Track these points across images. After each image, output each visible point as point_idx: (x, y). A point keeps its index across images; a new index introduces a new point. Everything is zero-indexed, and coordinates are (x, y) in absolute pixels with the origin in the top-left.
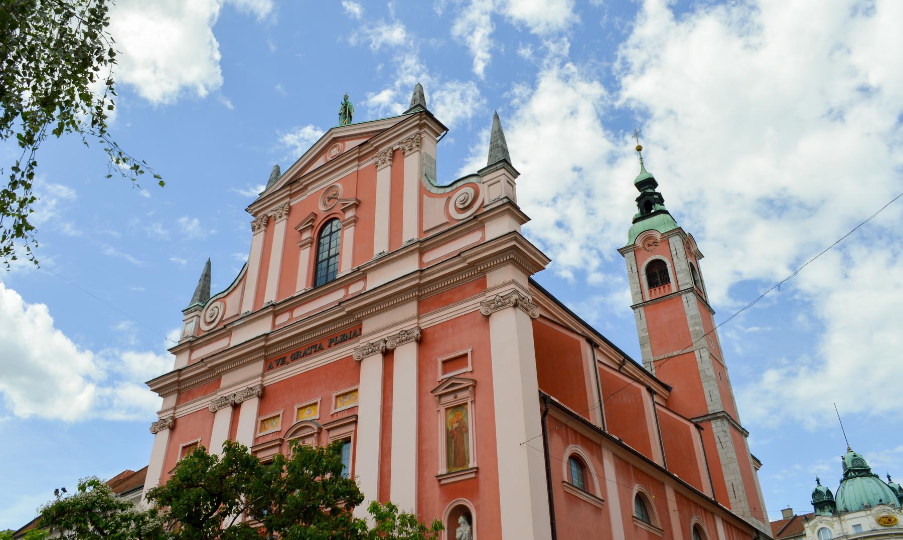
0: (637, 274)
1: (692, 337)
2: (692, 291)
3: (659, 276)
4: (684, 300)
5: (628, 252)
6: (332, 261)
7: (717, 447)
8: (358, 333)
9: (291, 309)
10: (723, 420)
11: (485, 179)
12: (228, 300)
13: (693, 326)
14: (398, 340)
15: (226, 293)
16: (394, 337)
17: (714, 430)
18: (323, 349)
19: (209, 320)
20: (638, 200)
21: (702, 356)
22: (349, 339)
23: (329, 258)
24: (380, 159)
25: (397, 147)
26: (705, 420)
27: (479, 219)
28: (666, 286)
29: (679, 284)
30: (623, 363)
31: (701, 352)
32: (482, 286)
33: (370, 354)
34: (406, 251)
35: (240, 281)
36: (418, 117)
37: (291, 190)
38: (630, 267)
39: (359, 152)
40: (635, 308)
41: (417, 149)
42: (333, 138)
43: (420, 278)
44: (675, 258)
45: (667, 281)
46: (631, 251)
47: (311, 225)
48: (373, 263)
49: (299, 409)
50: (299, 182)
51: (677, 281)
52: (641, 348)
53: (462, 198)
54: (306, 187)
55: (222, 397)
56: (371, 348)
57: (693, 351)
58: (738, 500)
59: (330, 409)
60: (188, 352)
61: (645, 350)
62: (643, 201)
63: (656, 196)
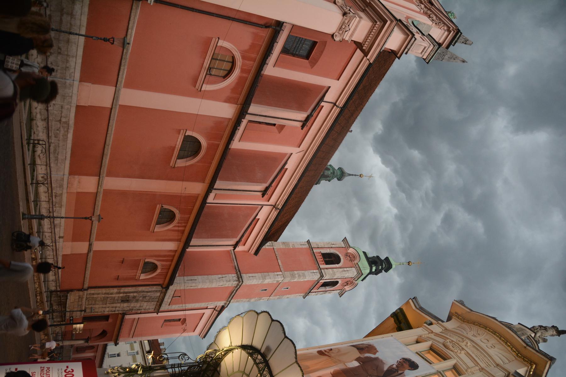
0: (330, 247)
1: (291, 272)
2: (321, 276)
3: (330, 260)
4: (315, 271)
5: (344, 244)
7: (219, 275)
10: (237, 281)
13: (298, 274)
17: (230, 275)
20: (378, 257)
21: (278, 276)
26: (236, 271)
28: (323, 262)
29: (325, 270)
30: (277, 209)
31: (281, 276)
38: (334, 243)
40: (308, 244)
44: (342, 269)
45: (327, 264)
46: (345, 245)
51: (327, 269)
52: (282, 242)
57: (281, 271)
58: (185, 281)
61: (281, 244)
62: (378, 261)
63: (380, 267)
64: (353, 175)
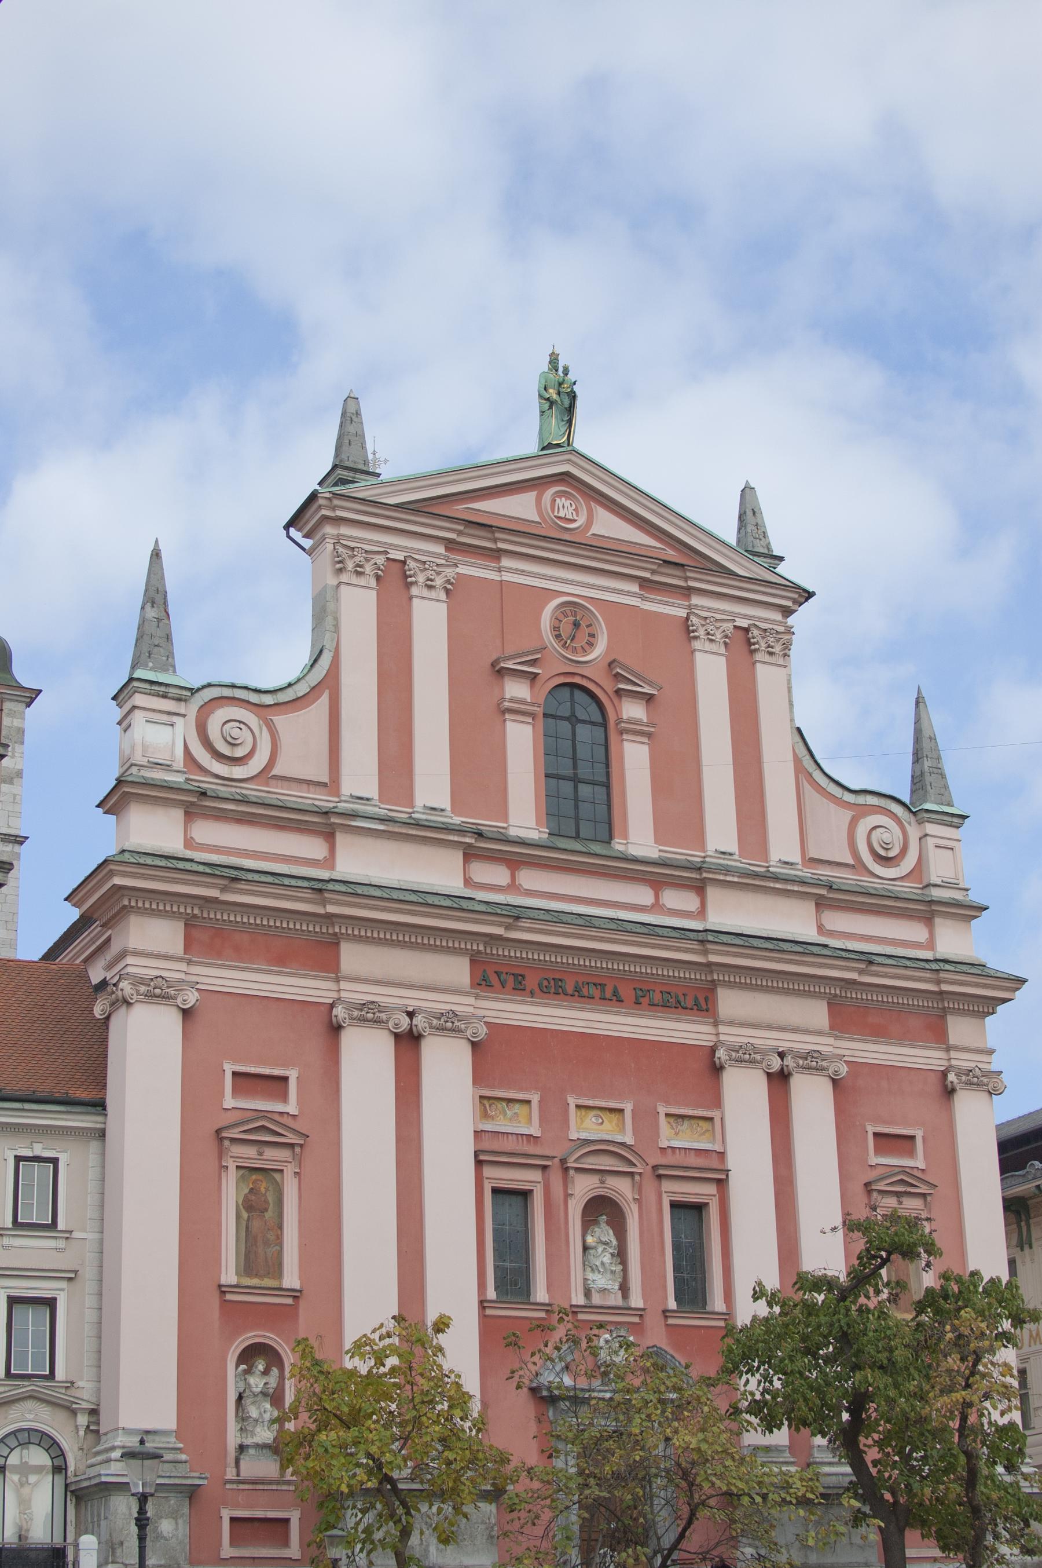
6: (585, 790)
8: (705, 1007)
9: (514, 863)
11: (931, 828)
12: (280, 721)
14: (801, 1062)
15: (268, 700)
16: (797, 1055)
18: (622, 1001)
22: (686, 1008)
23: (576, 780)
24: (703, 625)
25: (744, 623)
27: (934, 907)
32: (938, 1035)
33: (744, 1064)
34: (800, 889)
35: (315, 691)
36: (796, 596)
37: (460, 533)
39: (653, 572)
41: (781, 662)
42: (567, 474)
43: (861, 972)
47: (536, 675)
48: (733, 876)
49: (578, 1107)
50: (493, 532)
53: (886, 837)
54: (496, 554)
55: (373, 1002)
56: (750, 1054)
59: (657, 1134)
60: (178, 814)
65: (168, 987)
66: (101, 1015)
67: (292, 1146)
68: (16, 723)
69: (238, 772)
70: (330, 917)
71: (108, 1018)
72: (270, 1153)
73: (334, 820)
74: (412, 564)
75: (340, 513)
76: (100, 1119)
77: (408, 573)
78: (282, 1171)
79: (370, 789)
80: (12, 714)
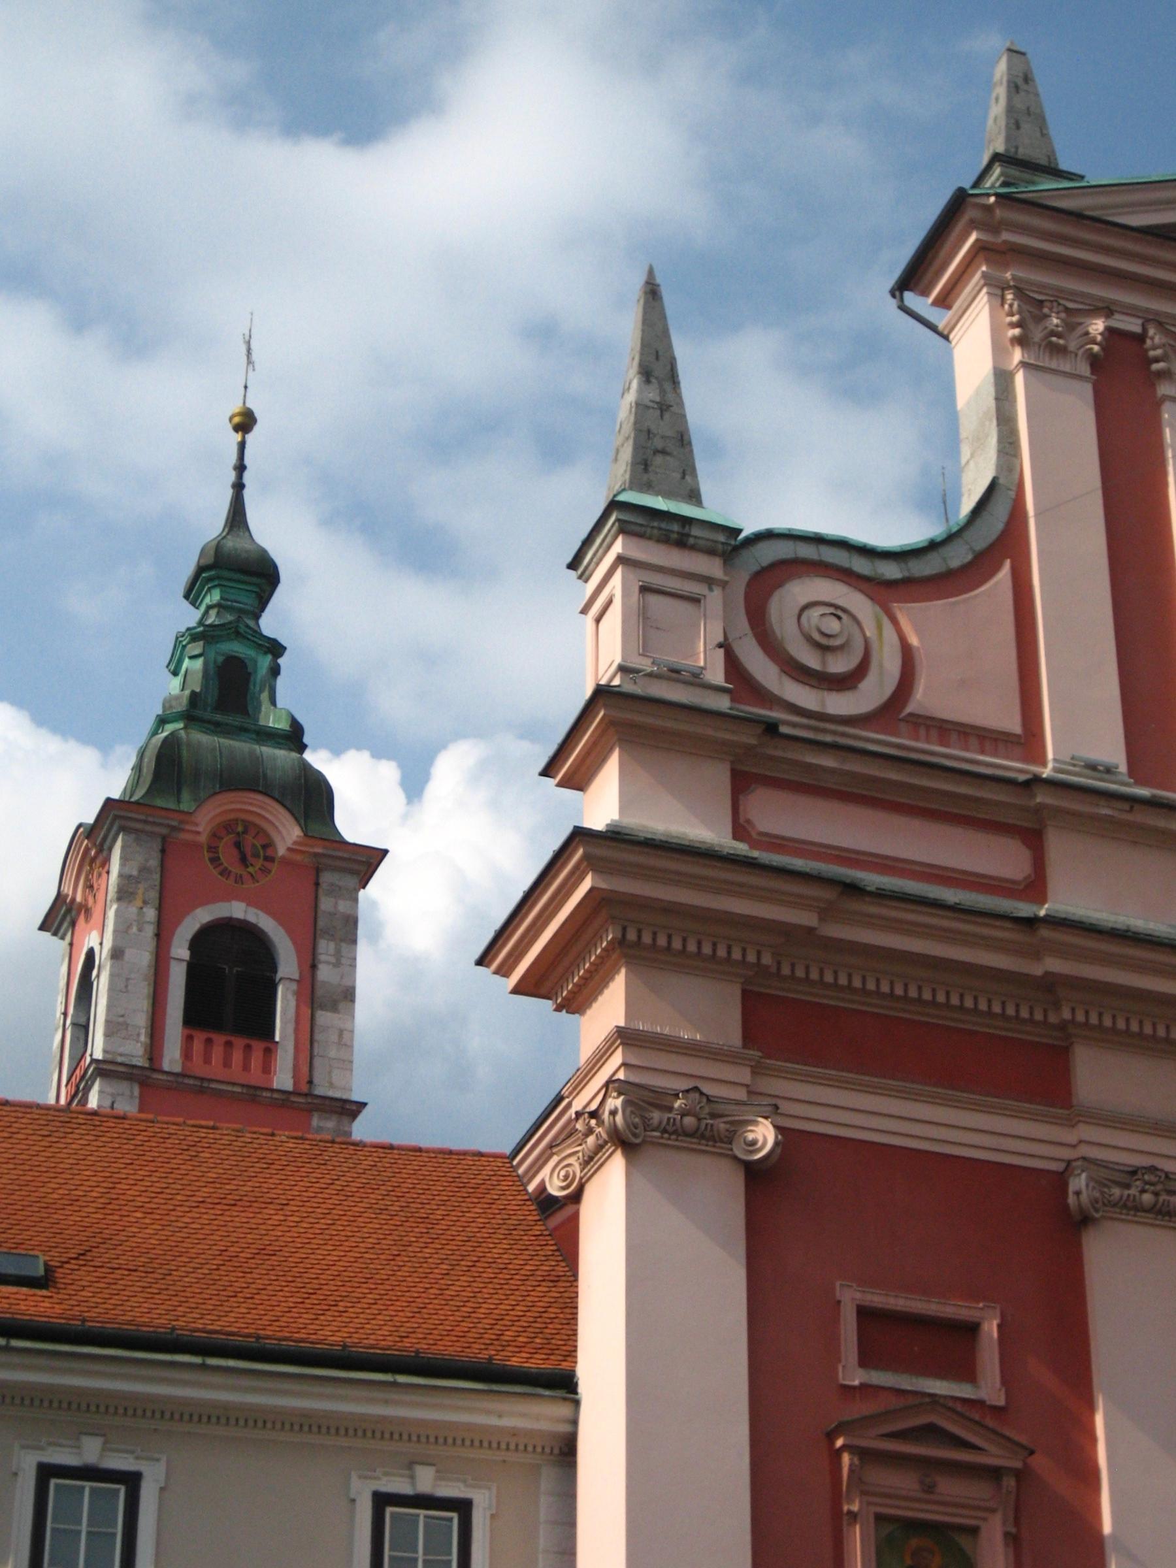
15: (891, 571)
19: (812, 660)
55: (1153, 1169)
60: (718, 776)
64: (239, 487)
65: (714, 1116)
66: (563, 1188)
67: (994, 1474)
68: (343, 906)
69: (839, 704)
70: (1050, 985)
71: (576, 1197)
72: (950, 1488)
73: (1042, 797)
74: (1155, 337)
75: (1006, 236)
76: (564, 1410)
77: (1152, 353)
78: (974, 1531)
79: (1112, 751)
80: (336, 891)
